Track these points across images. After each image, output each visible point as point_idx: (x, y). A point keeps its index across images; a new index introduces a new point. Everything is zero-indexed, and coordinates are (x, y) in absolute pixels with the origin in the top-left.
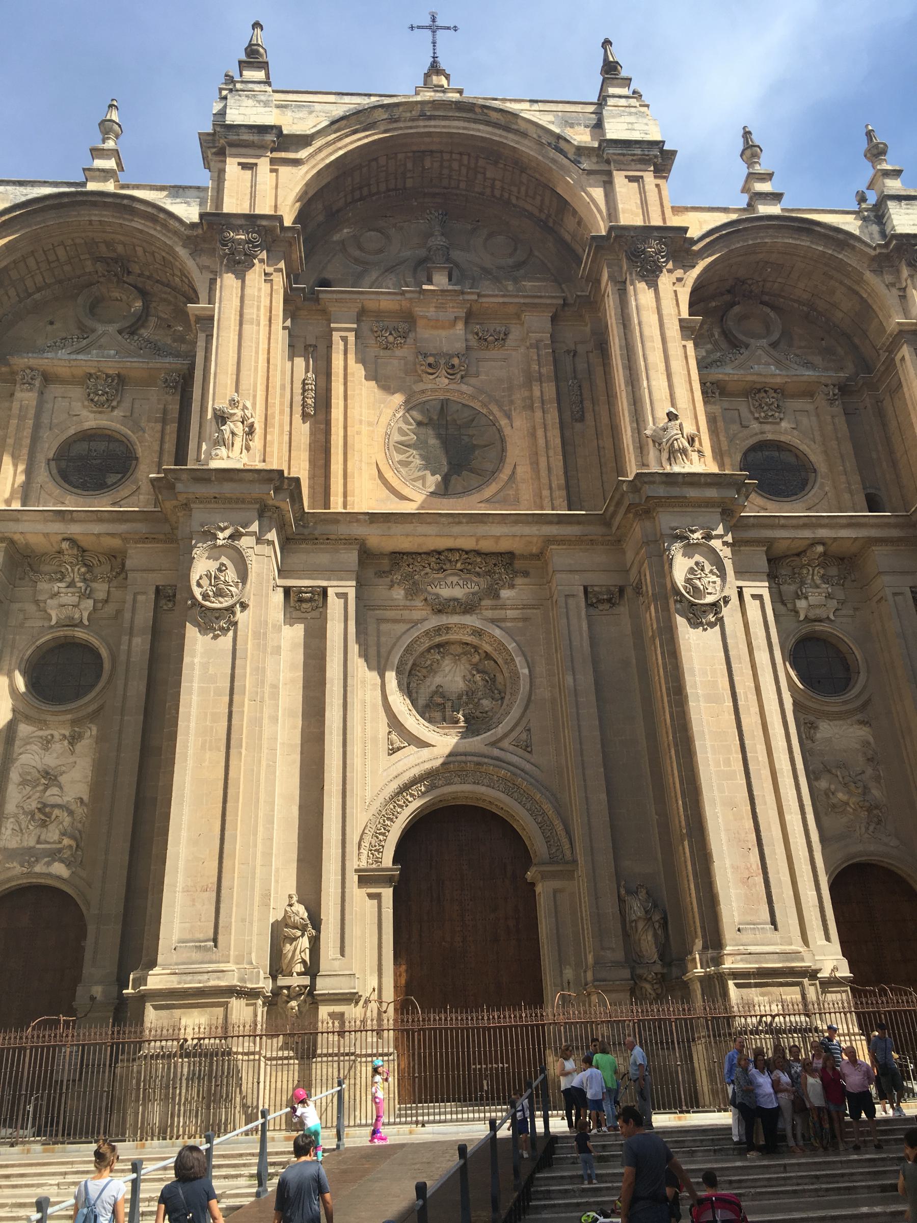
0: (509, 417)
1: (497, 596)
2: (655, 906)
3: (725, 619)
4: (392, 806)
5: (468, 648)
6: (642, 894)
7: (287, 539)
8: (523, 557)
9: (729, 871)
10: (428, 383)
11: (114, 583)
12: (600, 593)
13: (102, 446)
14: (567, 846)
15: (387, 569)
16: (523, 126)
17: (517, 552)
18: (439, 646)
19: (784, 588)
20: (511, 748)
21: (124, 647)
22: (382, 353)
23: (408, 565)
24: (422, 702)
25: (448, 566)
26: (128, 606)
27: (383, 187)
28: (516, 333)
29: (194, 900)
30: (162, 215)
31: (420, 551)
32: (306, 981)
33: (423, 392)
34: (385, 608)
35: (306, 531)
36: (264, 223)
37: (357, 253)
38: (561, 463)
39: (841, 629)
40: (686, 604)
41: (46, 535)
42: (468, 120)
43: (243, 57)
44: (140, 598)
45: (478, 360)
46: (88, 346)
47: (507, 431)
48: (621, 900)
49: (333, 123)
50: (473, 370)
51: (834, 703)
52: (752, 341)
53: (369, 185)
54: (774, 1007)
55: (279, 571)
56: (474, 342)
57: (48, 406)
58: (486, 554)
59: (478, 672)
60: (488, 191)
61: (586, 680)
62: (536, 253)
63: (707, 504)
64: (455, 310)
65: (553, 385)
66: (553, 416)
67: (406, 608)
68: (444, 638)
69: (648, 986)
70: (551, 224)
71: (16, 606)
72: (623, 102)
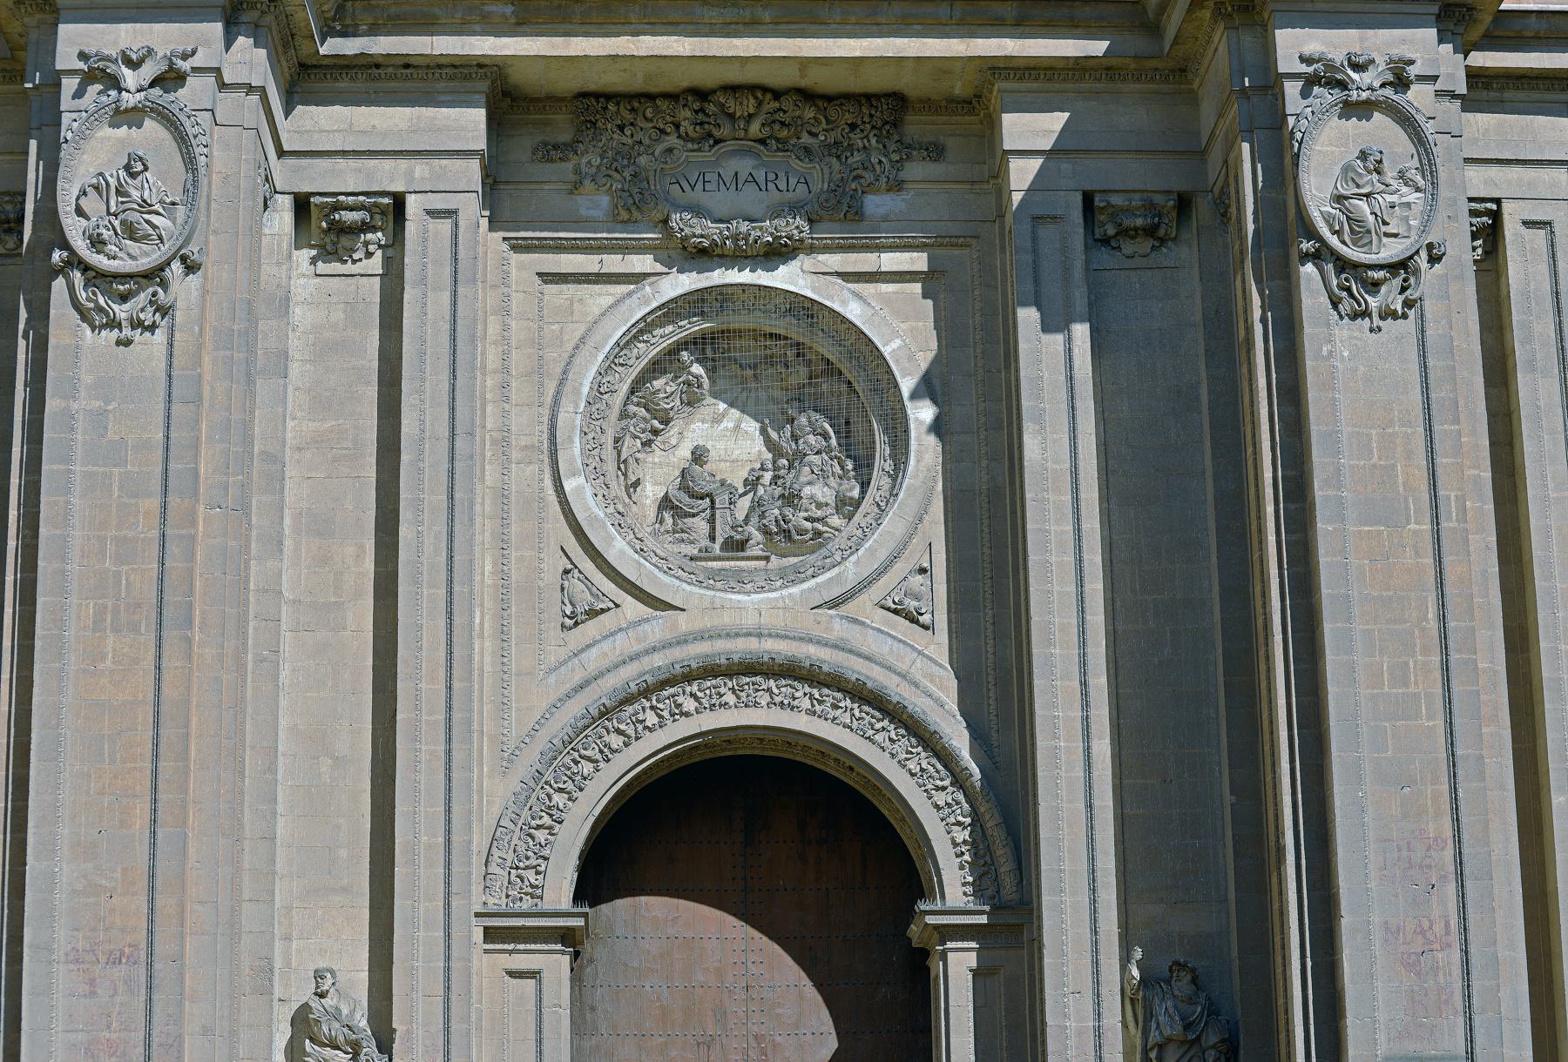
2: (1212, 1011)
3: (1427, 304)
4: (567, 760)
5: (776, 348)
6: (1182, 985)
7: (301, 65)
8: (929, 105)
9: (1377, 937)
12: (1128, 211)
15: (565, 137)
17: (912, 93)
20: (880, 618)
23: (621, 128)
24: (651, 492)
25: (725, 131)
29: (92, 982)
31: (653, 89)
55: (281, 153)
58: (829, 98)
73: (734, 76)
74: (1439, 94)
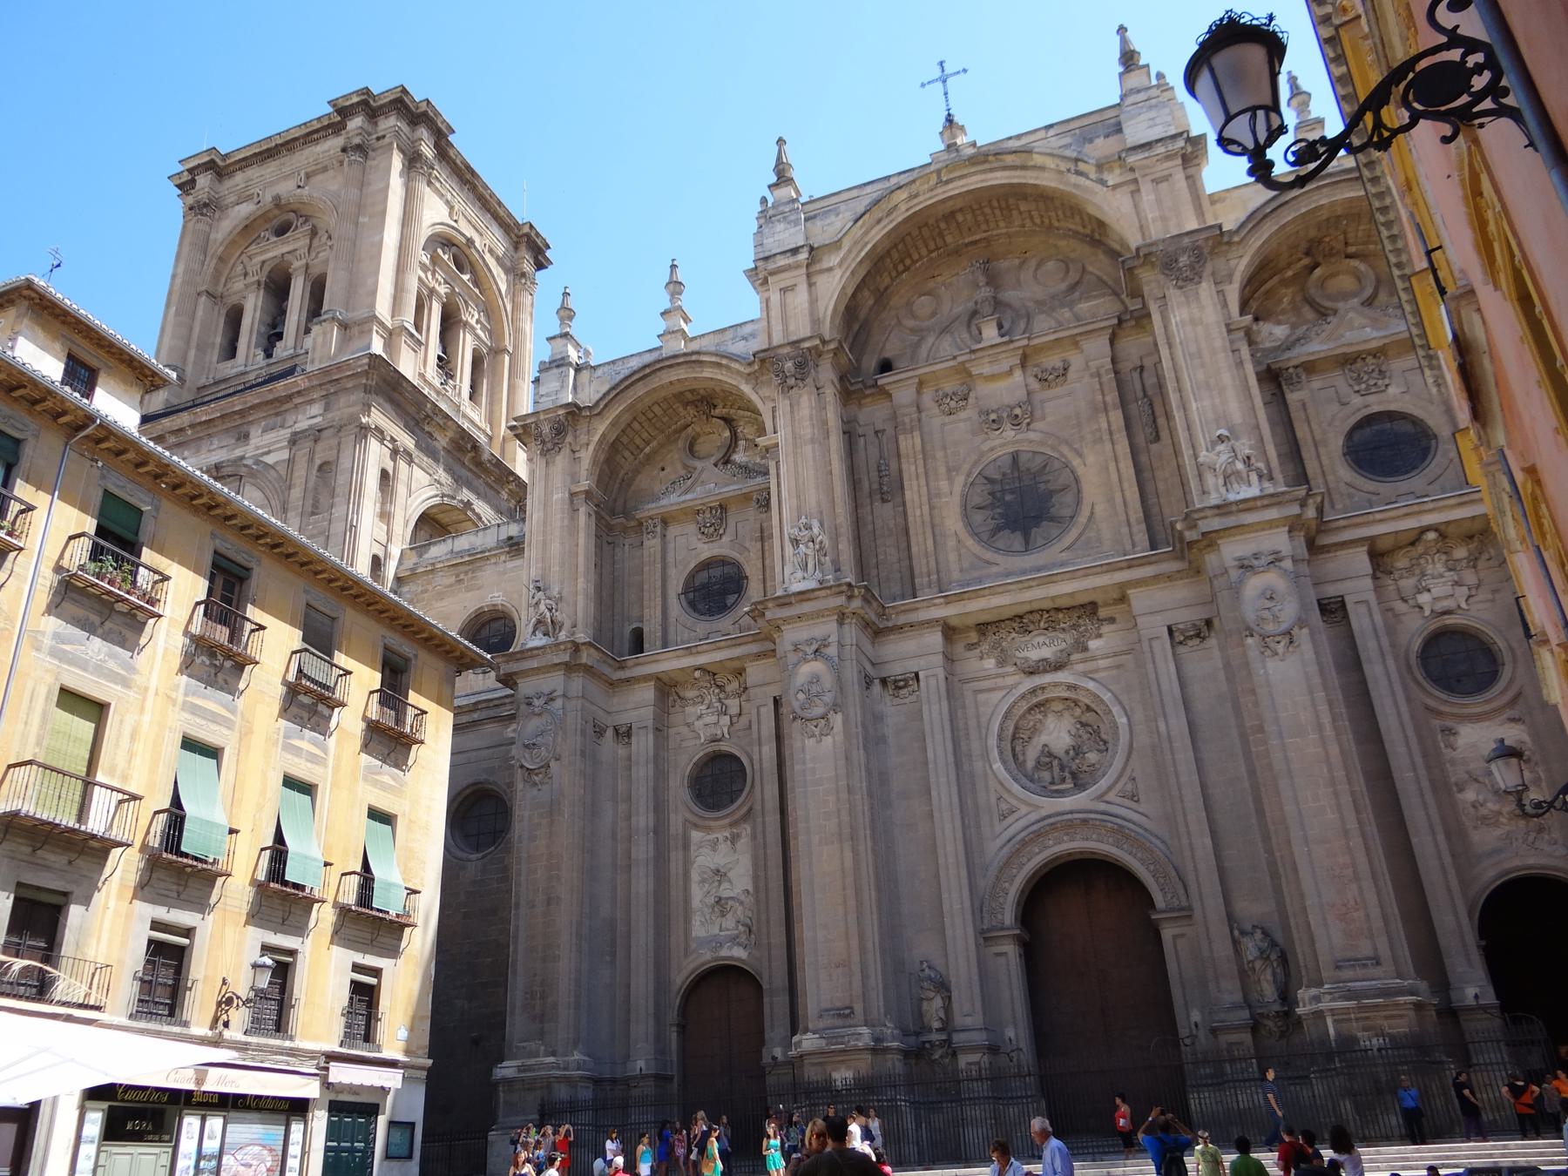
0: (1080, 455)
1: (1086, 649)
6: (1258, 935)
10: (995, 439)
11: (744, 697)
13: (716, 572)
14: (1182, 891)
16: (1038, 159)
18: (1038, 705)
19: (1403, 583)
20: (1119, 800)
21: (756, 757)
22: (947, 419)
24: (1030, 764)
26: (754, 719)
27: (924, 252)
28: (1076, 361)
30: (724, 362)
32: (944, 1037)
33: (992, 449)
34: (978, 679)
35: (890, 624)
36: (807, 345)
37: (911, 323)
38: (1137, 495)
39: (1479, 614)
40: (1257, 637)
41: (682, 669)
42: (984, 172)
43: (774, 179)
44: (763, 710)
45: (1043, 402)
46: (693, 484)
47: (1080, 471)
48: (1235, 942)
49: (856, 221)
50: (1038, 413)
51: (1476, 704)
52: (1340, 305)
53: (910, 256)
54: (1374, 1041)
55: (873, 664)
56: (1035, 385)
57: (671, 546)
59: (1083, 725)
60: (1028, 223)
61: (1178, 723)
62: (1090, 269)
63: (1271, 524)
64: (1009, 360)
65: (1119, 412)
66: (1123, 447)
67: (998, 676)
68: (1042, 698)
69: (1270, 1023)
70: (1097, 237)
71: (672, 731)
72: (1142, 96)
73: (1028, 608)
74: (1294, 561)
